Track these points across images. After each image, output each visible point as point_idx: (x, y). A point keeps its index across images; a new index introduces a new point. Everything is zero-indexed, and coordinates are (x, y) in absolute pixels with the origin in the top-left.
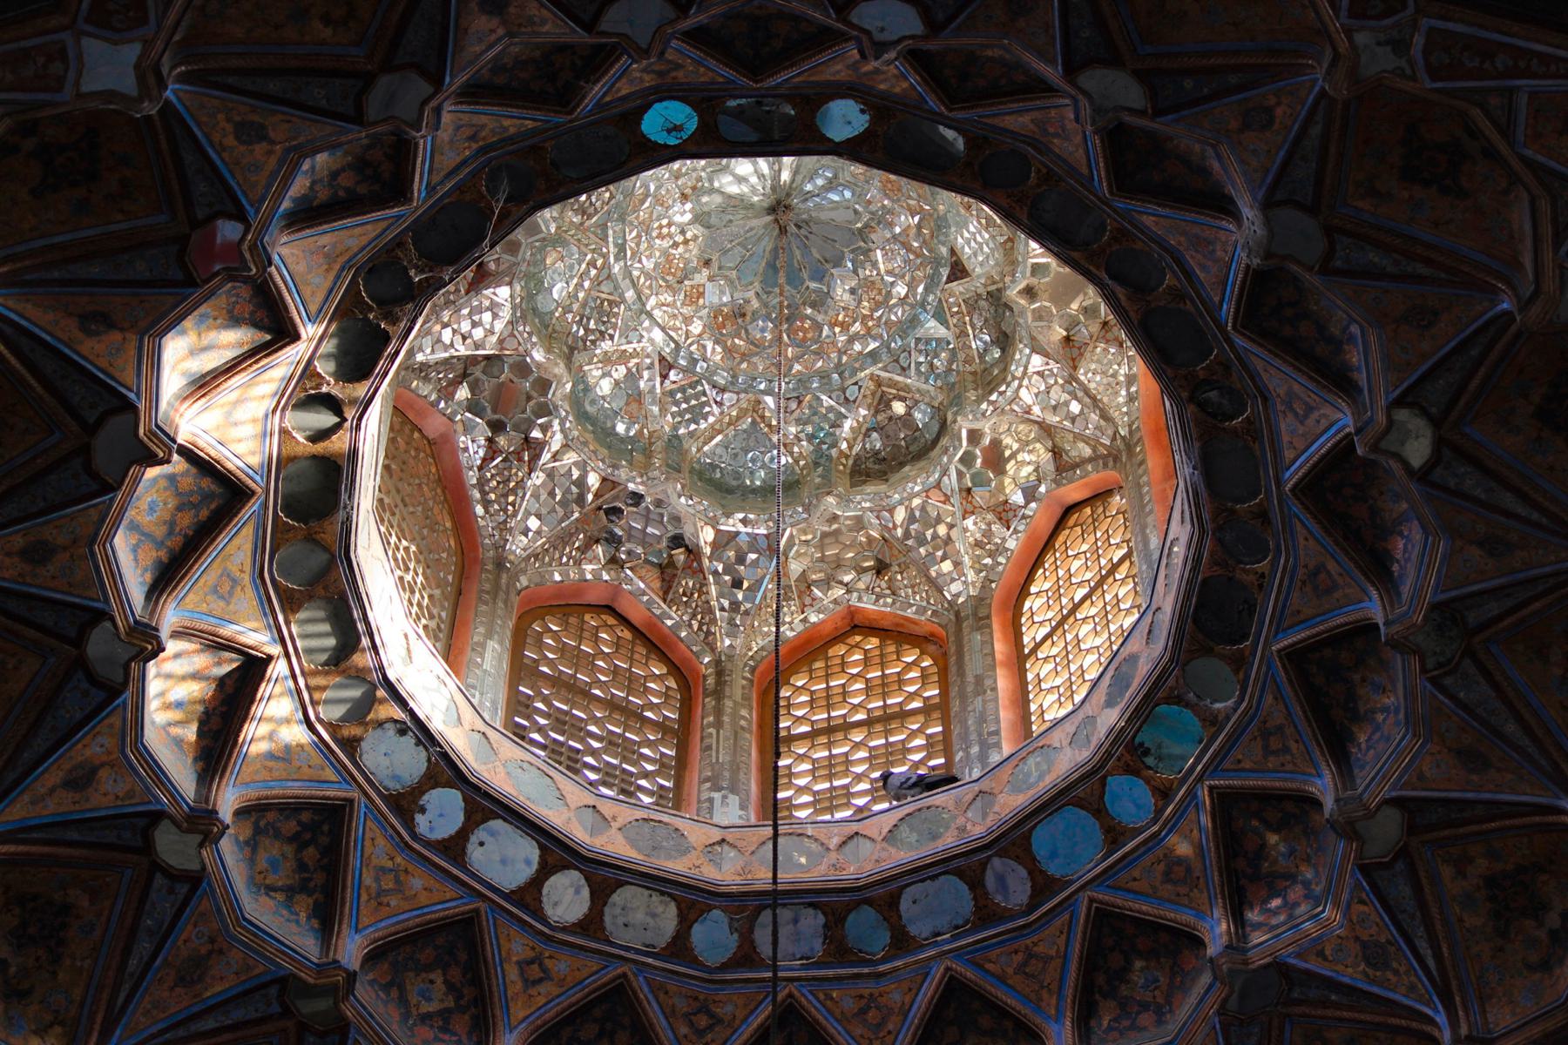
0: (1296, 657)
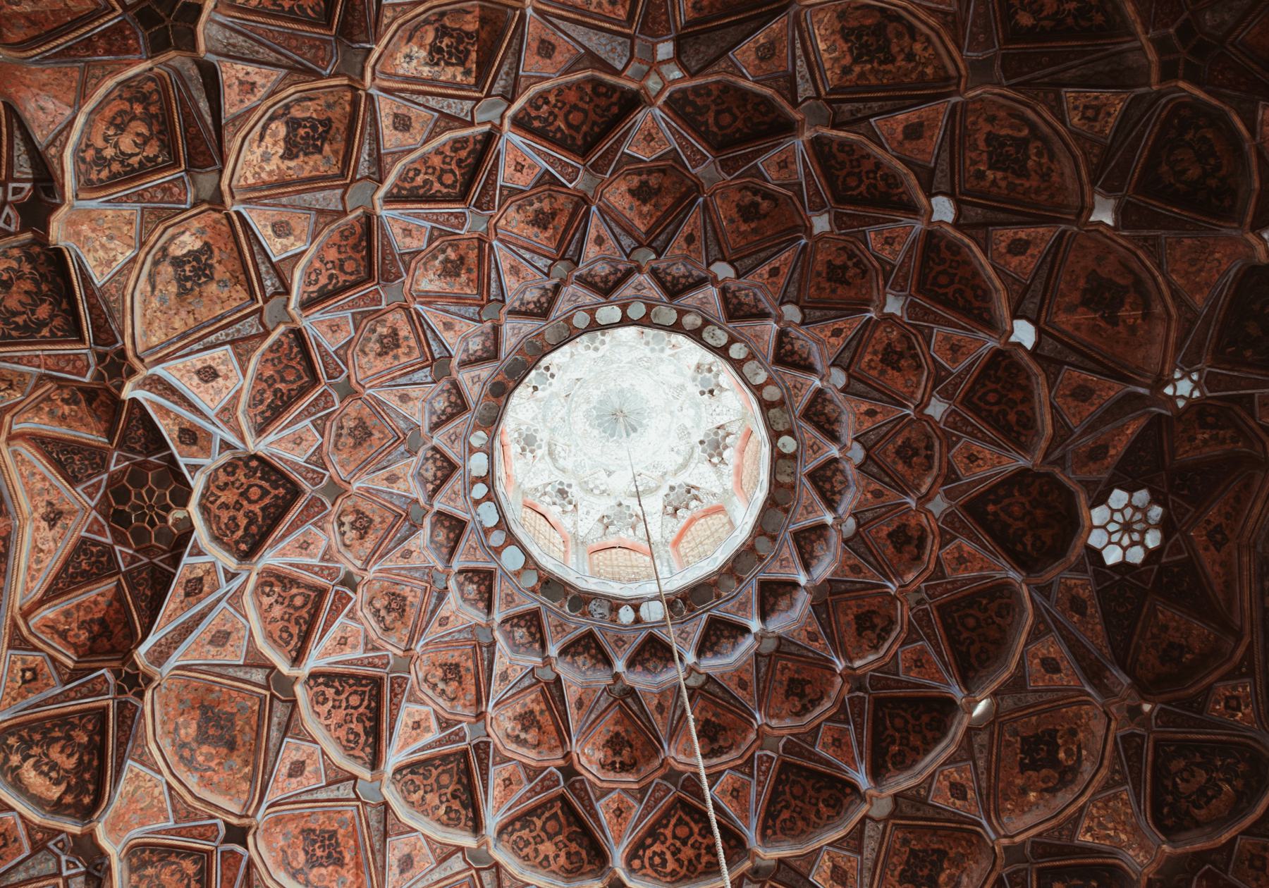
0: (590, 635)
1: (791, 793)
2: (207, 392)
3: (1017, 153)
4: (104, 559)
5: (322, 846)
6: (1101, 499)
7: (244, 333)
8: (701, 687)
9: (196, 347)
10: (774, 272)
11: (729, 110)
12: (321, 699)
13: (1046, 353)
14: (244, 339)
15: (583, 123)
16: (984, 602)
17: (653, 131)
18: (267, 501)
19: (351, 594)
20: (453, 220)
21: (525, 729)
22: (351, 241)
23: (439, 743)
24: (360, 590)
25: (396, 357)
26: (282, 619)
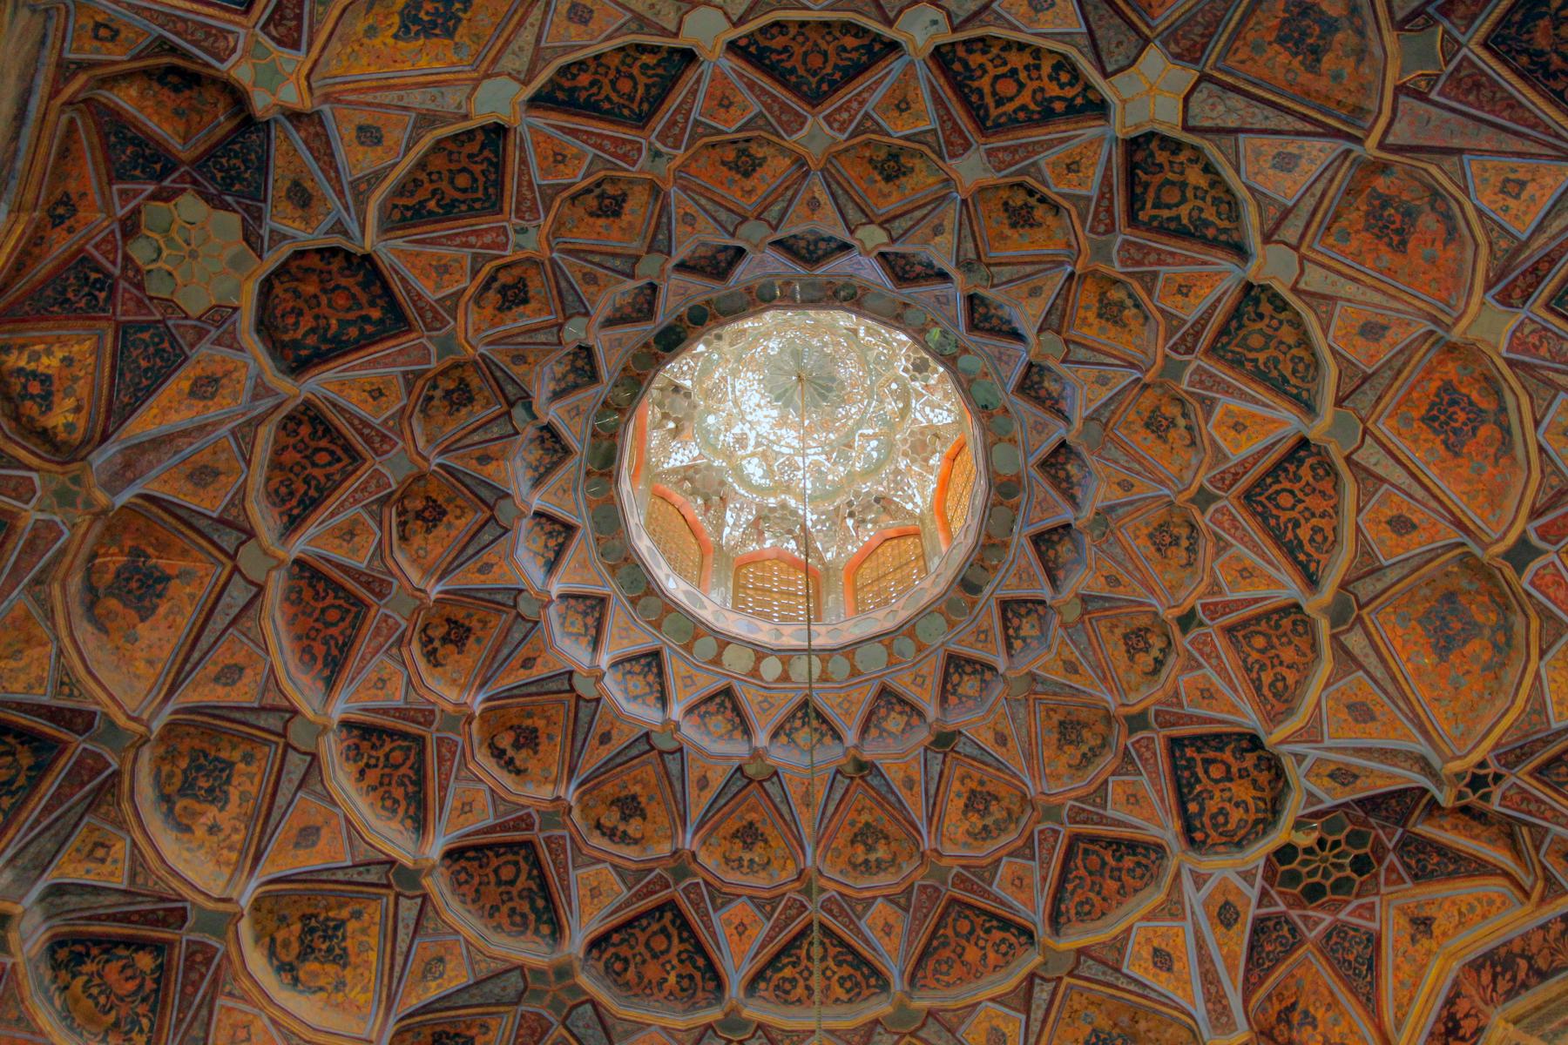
1: (826, 61)
2: (1176, 947)
3: (195, 779)
4: (1412, 848)
5: (1450, 418)
6: (221, 315)
7: (1101, 968)
8: (871, 222)
9: (1153, 995)
10: (527, 663)
11: (499, 883)
12: (1319, 538)
13: (235, 533)
14: (1105, 963)
15: (655, 933)
16: (432, 204)
17: (588, 900)
18: (1211, 754)
19: (1199, 608)
20: (836, 911)
21: (1121, 306)
22: (946, 953)
23: (1229, 390)
24: (1187, 607)
25: (982, 783)
26: (1290, 643)
